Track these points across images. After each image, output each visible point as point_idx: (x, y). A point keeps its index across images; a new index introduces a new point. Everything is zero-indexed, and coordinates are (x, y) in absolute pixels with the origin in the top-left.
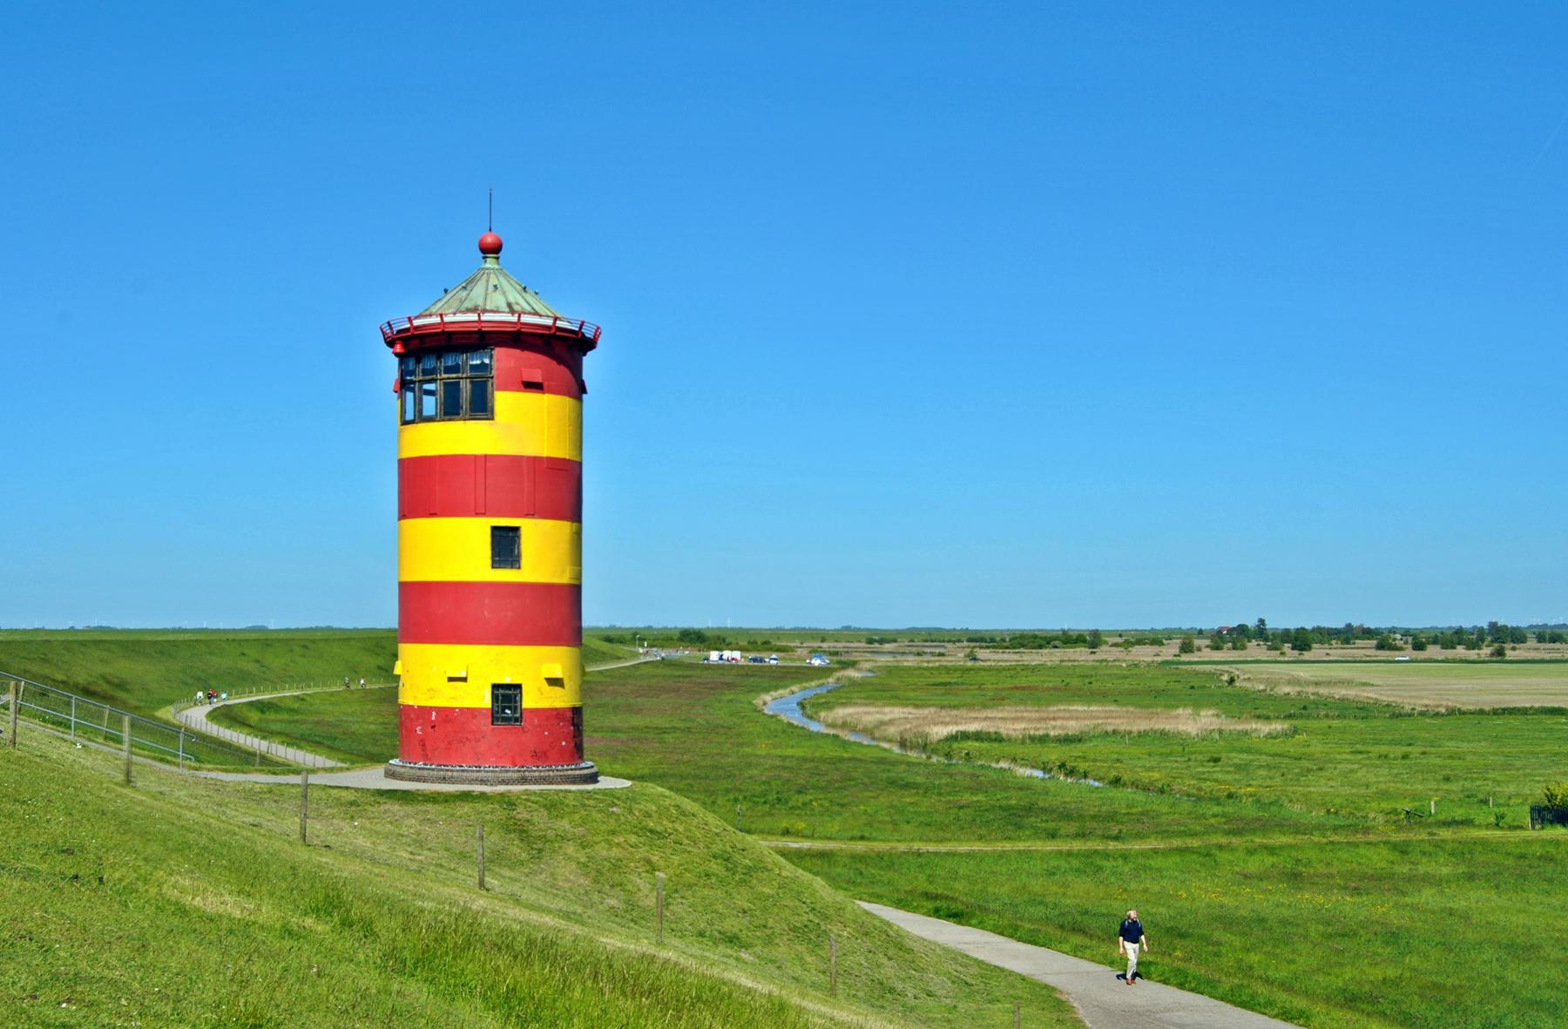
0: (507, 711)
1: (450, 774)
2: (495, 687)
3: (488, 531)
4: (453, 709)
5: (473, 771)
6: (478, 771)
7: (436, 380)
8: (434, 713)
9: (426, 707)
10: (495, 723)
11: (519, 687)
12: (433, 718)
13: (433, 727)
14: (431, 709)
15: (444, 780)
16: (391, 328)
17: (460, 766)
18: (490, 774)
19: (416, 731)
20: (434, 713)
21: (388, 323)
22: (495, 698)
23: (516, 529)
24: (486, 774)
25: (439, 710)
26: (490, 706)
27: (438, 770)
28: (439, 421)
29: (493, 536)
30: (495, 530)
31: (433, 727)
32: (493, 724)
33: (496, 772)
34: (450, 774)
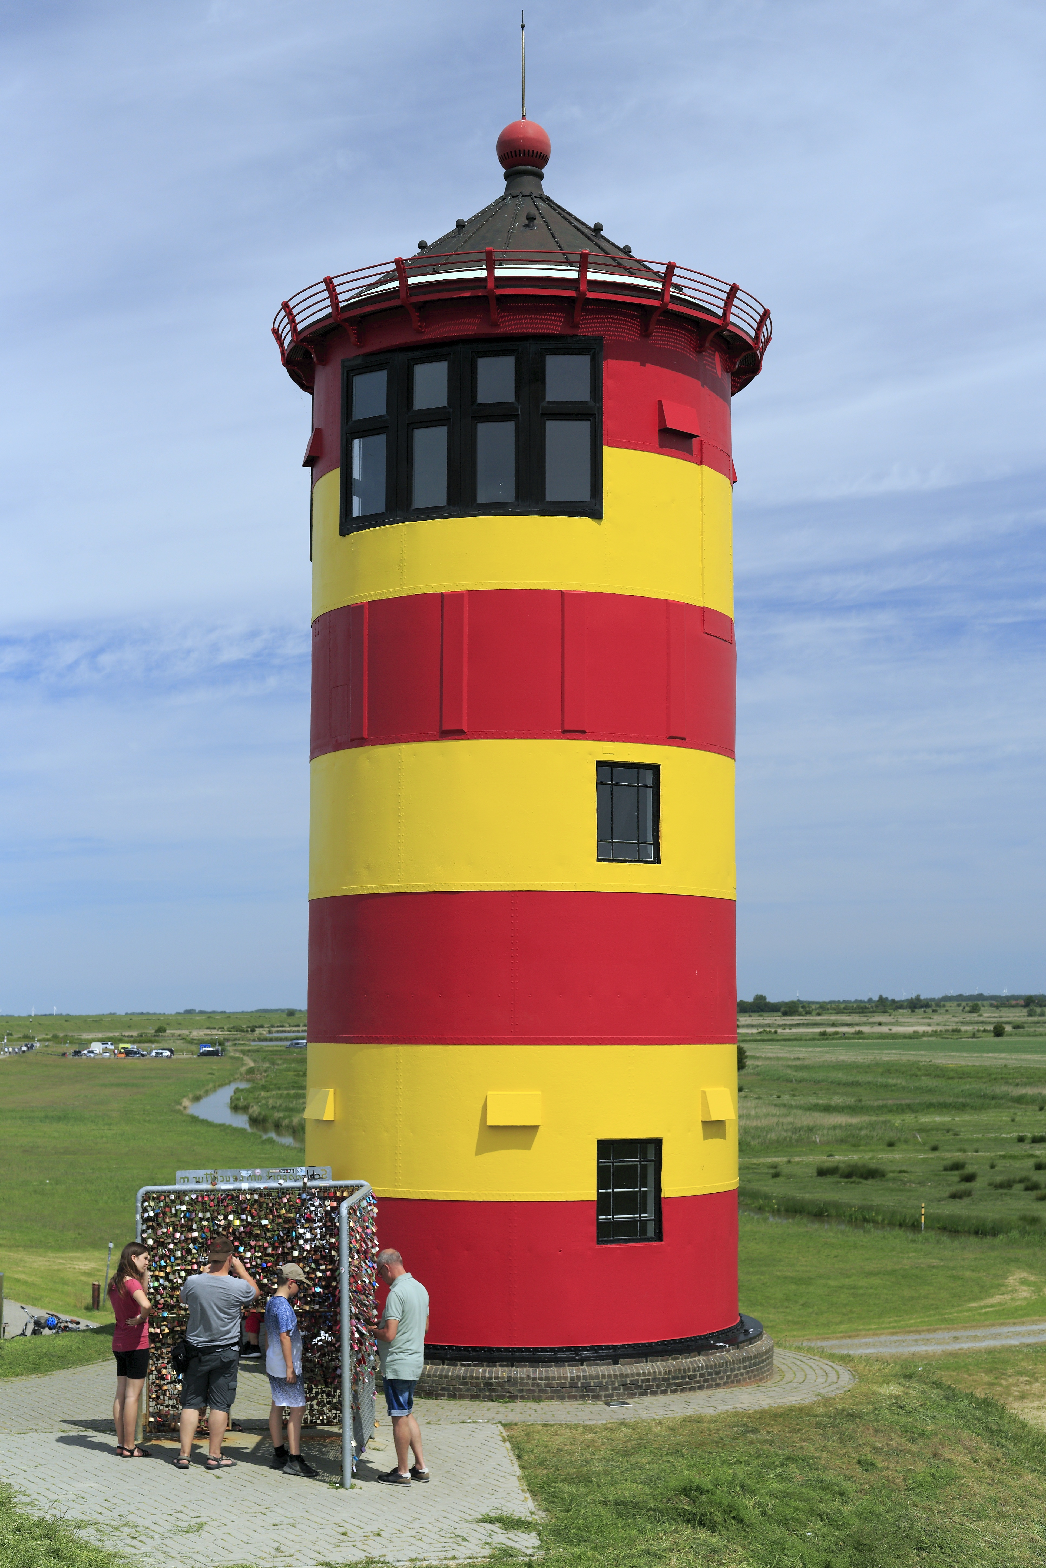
2: (606, 1148)
16: (333, 295)
21: (328, 282)
22: (604, 1177)
23: (655, 769)
29: (600, 785)
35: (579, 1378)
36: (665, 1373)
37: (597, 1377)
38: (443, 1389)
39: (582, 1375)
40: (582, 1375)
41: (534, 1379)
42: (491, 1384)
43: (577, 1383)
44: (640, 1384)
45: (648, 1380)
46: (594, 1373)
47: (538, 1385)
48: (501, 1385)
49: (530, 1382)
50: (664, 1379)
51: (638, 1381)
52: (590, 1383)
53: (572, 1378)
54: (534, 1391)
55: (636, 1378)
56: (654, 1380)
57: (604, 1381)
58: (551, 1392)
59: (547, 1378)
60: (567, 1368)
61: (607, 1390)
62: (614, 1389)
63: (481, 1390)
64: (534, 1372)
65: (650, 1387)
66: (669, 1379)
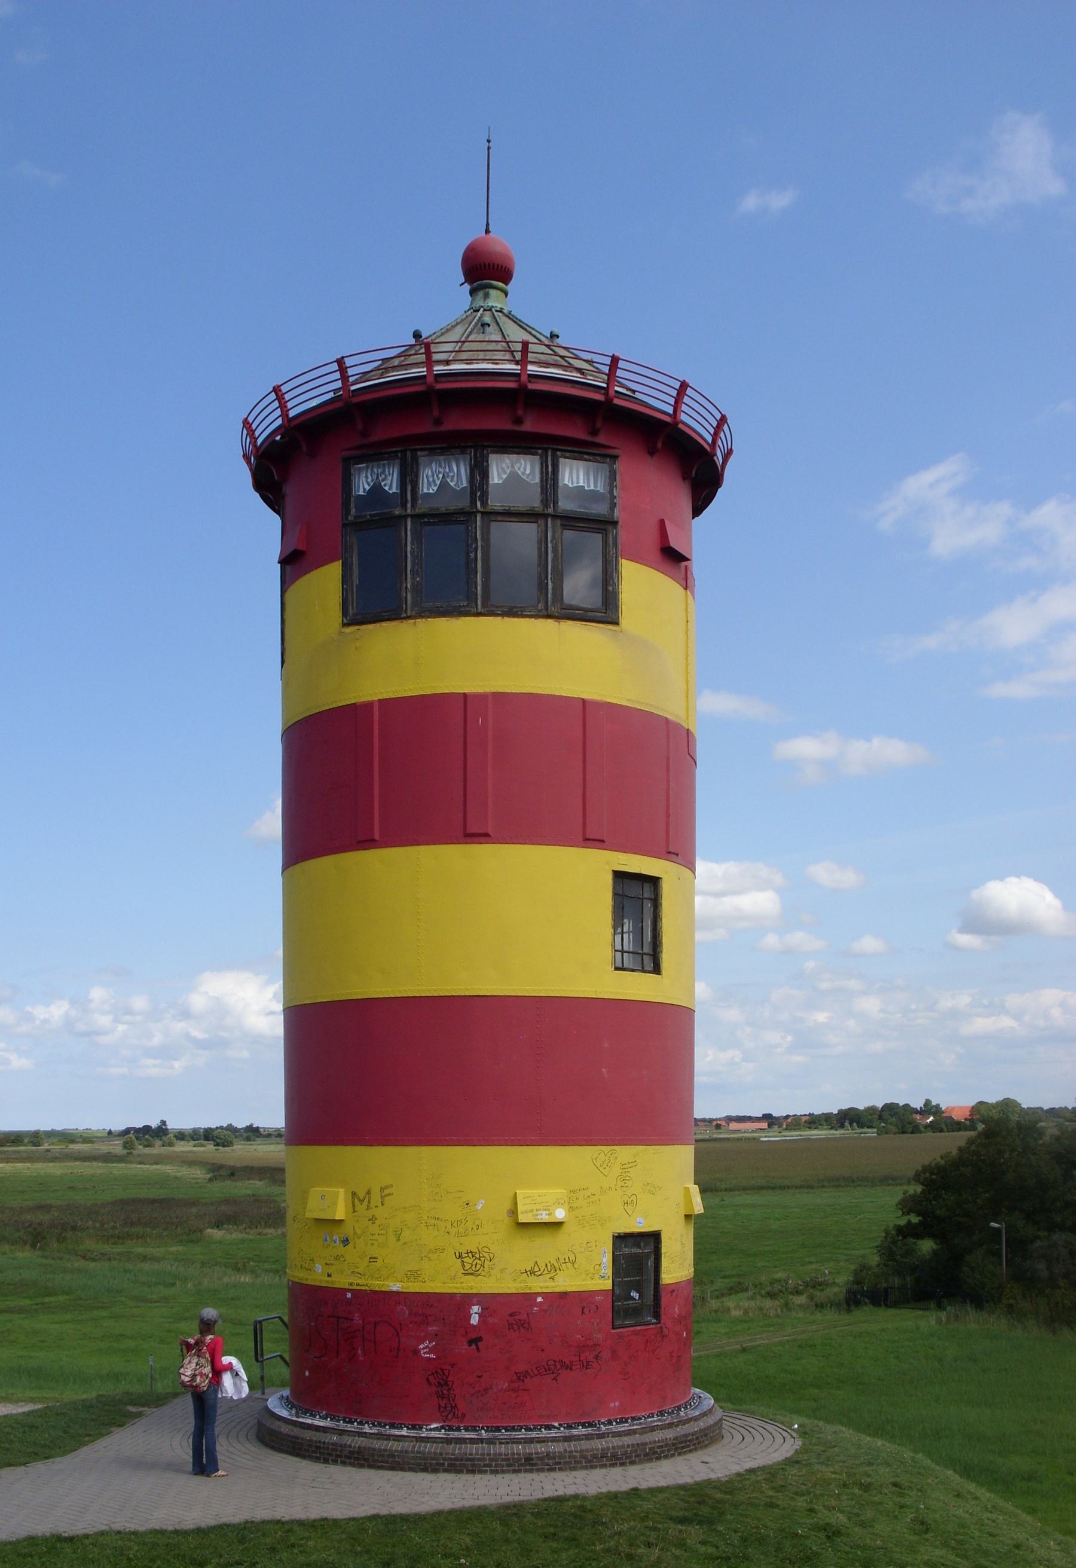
0: (635, 1295)
1: (541, 1448)
2: (620, 1239)
3: (609, 878)
4: (529, 1297)
5: (578, 1438)
6: (588, 1437)
7: (474, 514)
8: (476, 1309)
9: (452, 1296)
10: (618, 1323)
11: (655, 1237)
12: (475, 1320)
13: (475, 1341)
14: (467, 1300)
15: (529, 1464)
17: (549, 1427)
18: (627, 1440)
19: (416, 1352)
20: (476, 1309)
24: (616, 1442)
25: (491, 1302)
26: (607, 1284)
27: (491, 1441)
28: (479, 614)
30: (620, 876)
31: (475, 1341)
32: (613, 1328)
33: (634, 1432)
34: (541, 1448)
35: (608, 1448)
36: (674, 1439)
37: (623, 1446)
38: (485, 1466)
39: (611, 1445)
40: (611, 1445)
41: (571, 1452)
42: (532, 1459)
43: (607, 1453)
44: (656, 1450)
45: (661, 1447)
46: (620, 1443)
47: (575, 1457)
48: (542, 1459)
49: (567, 1455)
50: (674, 1444)
51: (654, 1447)
52: (617, 1452)
53: (603, 1449)
54: (570, 1463)
55: (653, 1445)
56: (666, 1445)
57: (629, 1449)
58: (585, 1463)
59: (581, 1451)
60: (597, 1441)
61: (630, 1457)
62: (637, 1456)
63: (521, 1465)
64: (570, 1446)
65: (663, 1452)
66: (676, 1443)
